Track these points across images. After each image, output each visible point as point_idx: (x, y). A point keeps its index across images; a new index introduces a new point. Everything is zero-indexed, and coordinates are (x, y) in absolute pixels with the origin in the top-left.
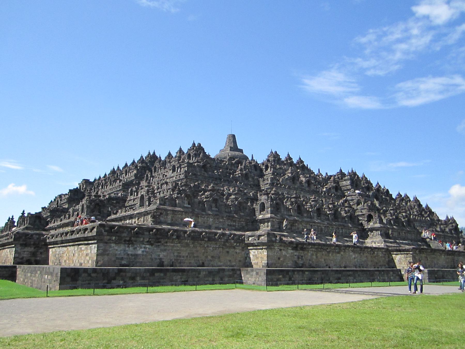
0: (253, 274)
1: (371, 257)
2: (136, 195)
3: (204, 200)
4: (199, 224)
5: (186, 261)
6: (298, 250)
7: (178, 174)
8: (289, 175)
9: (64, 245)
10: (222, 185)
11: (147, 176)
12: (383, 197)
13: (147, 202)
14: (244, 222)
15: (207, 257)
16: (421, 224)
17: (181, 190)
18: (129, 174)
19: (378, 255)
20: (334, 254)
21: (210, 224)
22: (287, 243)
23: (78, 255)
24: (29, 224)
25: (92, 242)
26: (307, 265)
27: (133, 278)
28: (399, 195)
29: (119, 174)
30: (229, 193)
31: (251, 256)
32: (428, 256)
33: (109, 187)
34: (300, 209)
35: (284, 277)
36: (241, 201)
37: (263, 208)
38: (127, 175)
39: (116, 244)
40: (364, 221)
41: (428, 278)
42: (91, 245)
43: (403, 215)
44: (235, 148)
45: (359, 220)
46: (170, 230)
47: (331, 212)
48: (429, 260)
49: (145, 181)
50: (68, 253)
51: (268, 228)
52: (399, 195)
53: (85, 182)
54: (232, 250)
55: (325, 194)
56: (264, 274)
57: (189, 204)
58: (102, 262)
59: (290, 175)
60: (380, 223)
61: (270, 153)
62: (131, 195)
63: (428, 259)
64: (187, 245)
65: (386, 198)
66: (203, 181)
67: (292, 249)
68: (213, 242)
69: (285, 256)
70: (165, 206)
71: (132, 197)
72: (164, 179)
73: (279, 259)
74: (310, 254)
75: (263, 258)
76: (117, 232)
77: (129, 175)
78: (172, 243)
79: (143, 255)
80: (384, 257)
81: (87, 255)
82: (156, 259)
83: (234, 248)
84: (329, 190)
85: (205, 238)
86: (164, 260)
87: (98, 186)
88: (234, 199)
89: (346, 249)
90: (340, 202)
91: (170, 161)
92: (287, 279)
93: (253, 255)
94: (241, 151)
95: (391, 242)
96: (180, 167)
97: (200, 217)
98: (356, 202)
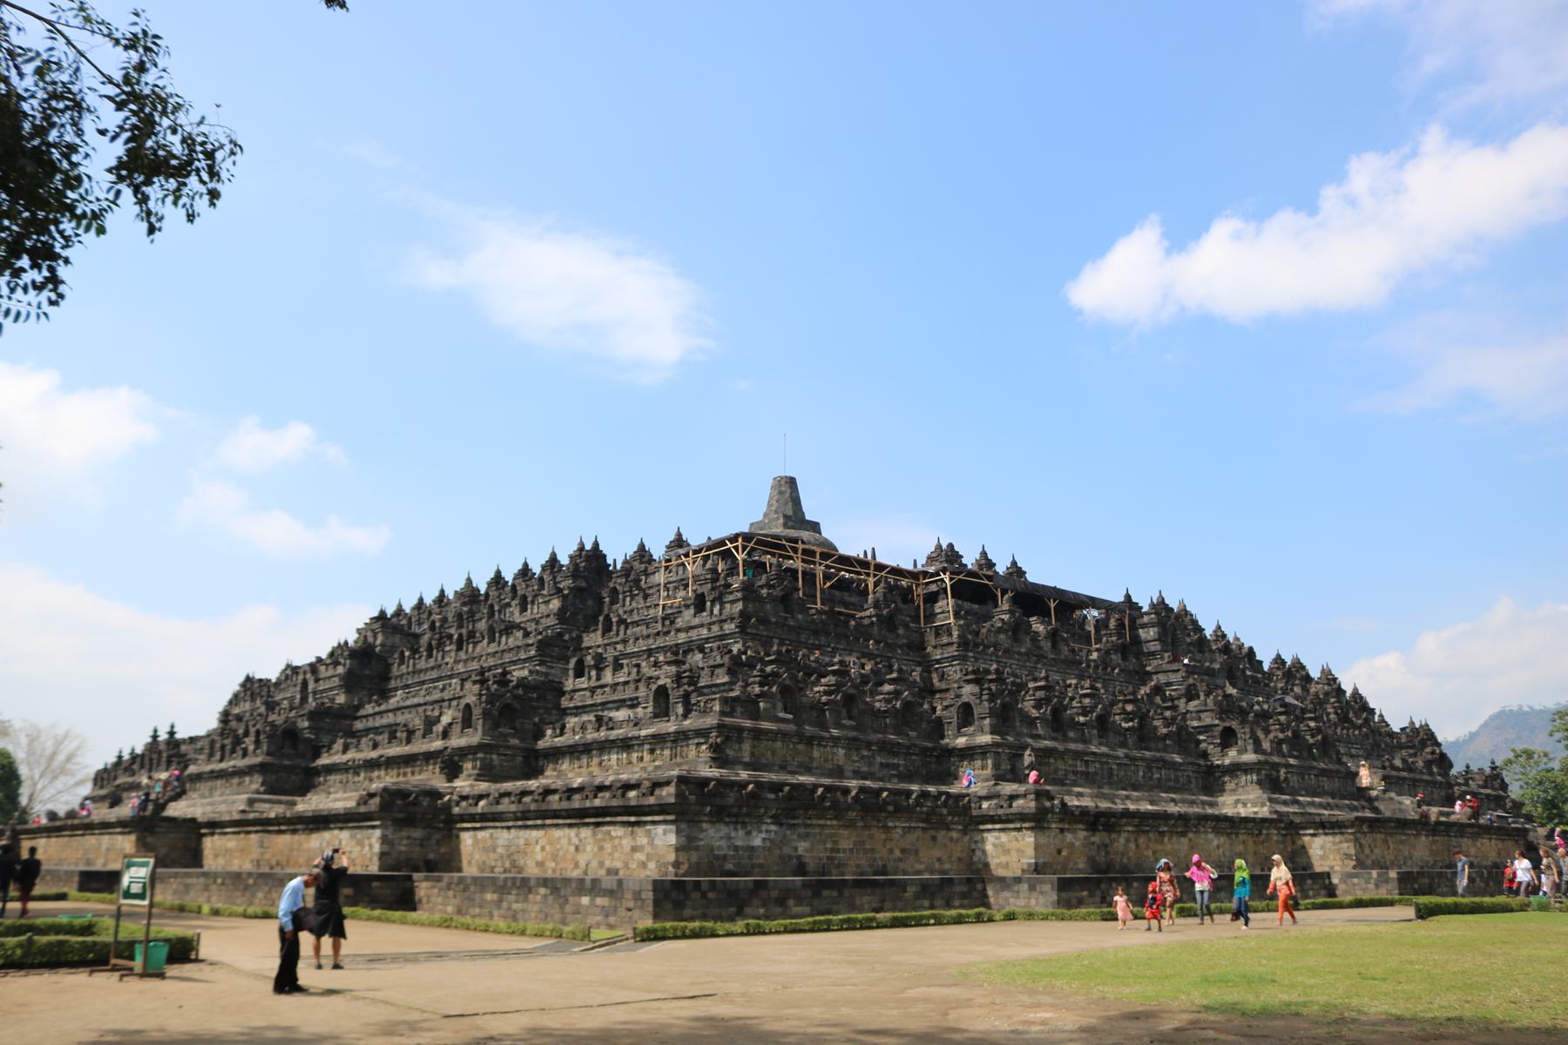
0: (1021, 889)
1: (1255, 842)
2: (594, 678)
3: (824, 699)
4: (815, 765)
5: (852, 862)
6: (1098, 830)
7: (714, 619)
8: (1003, 617)
9: (530, 823)
10: (830, 649)
11: (608, 619)
12: (1248, 673)
13: (680, 705)
14: (917, 755)
15: (891, 851)
16: (1350, 748)
17: (769, 675)
18: (532, 608)
20: (1174, 838)
21: (840, 763)
22: (1077, 813)
23: (596, 849)
24: (268, 754)
25: (657, 818)
26: (1117, 867)
27: (781, 902)
28: (1279, 660)
29: (496, 608)
30: (862, 676)
31: (989, 847)
32: (1389, 838)
33: (483, 647)
34: (1058, 722)
35: (1091, 895)
36: (909, 698)
37: (966, 715)
38: (526, 610)
39: (712, 822)
40: (1212, 746)
41: (1397, 891)
42: (648, 827)
43: (1308, 726)
44: (795, 516)
45: (1199, 742)
46: (815, 787)
47: (1131, 724)
48: (1392, 847)
49: (599, 633)
50: (550, 843)
51: (985, 772)
52: (1279, 660)
53: (383, 626)
54: (943, 832)
55: (1096, 667)
56: (1052, 889)
57: (786, 712)
58: (685, 867)
59: (1006, 617)
60: (1256, 752)
61: (933, 550)
62: (579, 673)
63: (1389, 848)
64: (851, 825)
65: (1256, 677)
66: (784, 640)
67: (1086, 830)
68: (906, 815)
69: (1072, 845)
70: (733, 717)
71: (583, 683)
72: (665, 630)
73: (1059, 852)
74: (1122, 840)
75: (1023, 852)
76: (715, 795)
77: (534, 611)
78: (821, 819)
79: (764, 848)
80: (1283, 842)
81: (634, 849)
82: (790, 857)
83: (948, 829)
85: (888, 804)
86: (806, 860)
87: (440, 645)
88: (889, 693)
89: (1199, 824)
90: (1142, 692)
91: (646, 568)
92: (1098, 899)
93: (995, 845)
94: (815, 527)
95: (1285, 803)
96: (719, 599)
97: (815, 747)
98: (1184, 692)
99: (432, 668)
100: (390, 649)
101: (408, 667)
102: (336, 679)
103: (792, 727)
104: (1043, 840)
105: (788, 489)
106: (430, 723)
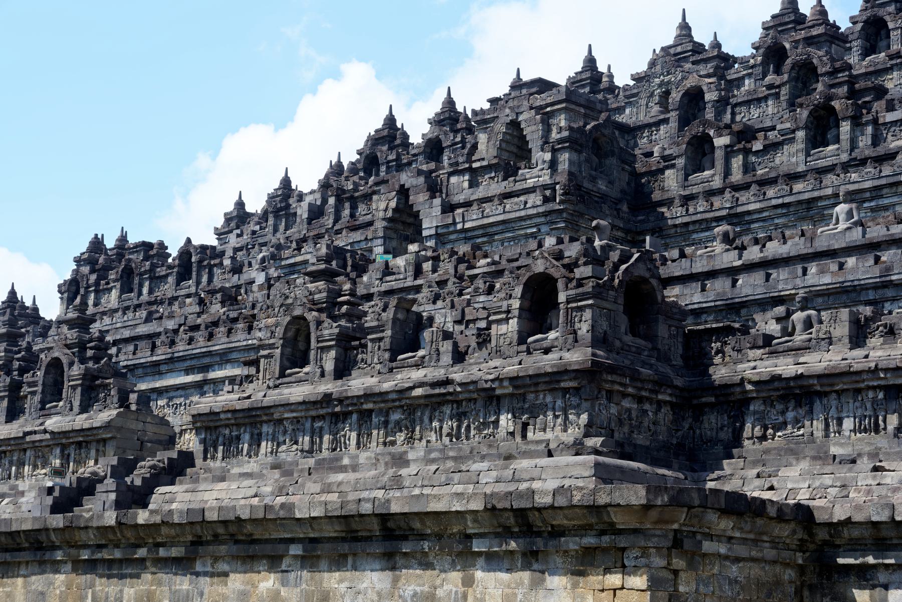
99: (846, 167)
101: (727, 173)
102: (535, 199)
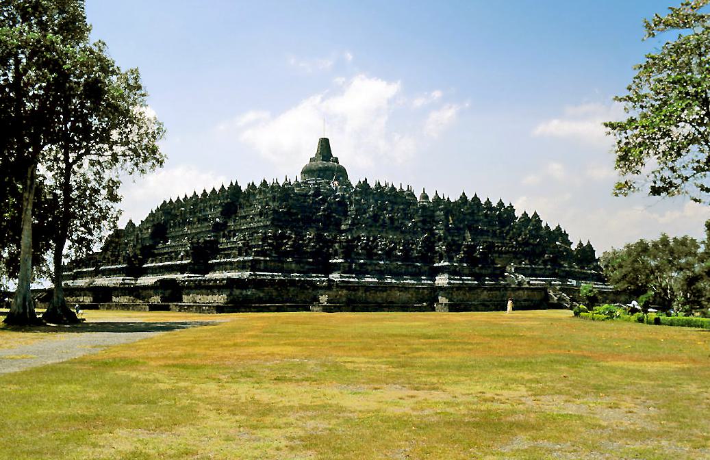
19: (423, 293)
28: (525, 214)
52: (525, 214)
69: (341, 295)
73: (336, 296)
83: (307, 289)
84: (415, 224)
94: (336, 160)
100: (166, 222)
103: (277, 259)
104: (331, 293)
105: (325, 144)
106: (177, 254)
